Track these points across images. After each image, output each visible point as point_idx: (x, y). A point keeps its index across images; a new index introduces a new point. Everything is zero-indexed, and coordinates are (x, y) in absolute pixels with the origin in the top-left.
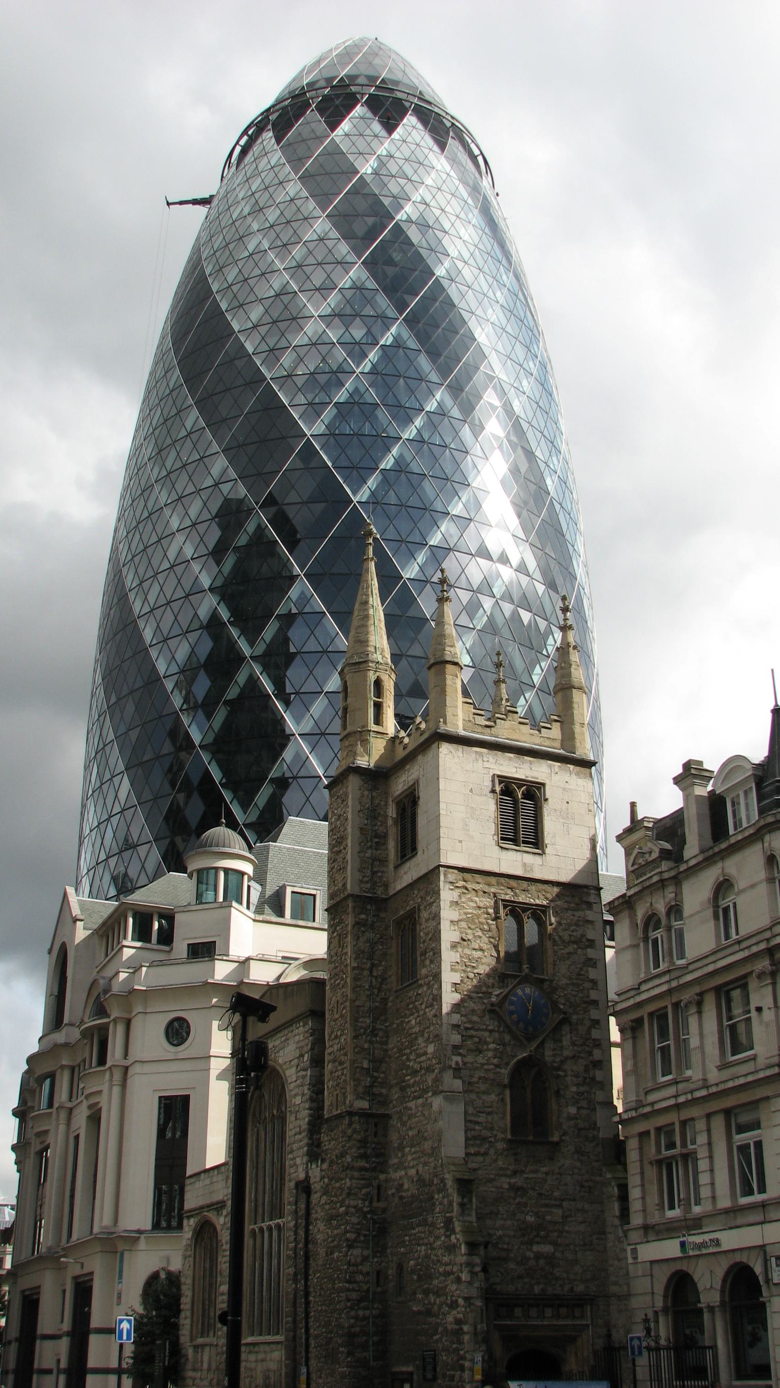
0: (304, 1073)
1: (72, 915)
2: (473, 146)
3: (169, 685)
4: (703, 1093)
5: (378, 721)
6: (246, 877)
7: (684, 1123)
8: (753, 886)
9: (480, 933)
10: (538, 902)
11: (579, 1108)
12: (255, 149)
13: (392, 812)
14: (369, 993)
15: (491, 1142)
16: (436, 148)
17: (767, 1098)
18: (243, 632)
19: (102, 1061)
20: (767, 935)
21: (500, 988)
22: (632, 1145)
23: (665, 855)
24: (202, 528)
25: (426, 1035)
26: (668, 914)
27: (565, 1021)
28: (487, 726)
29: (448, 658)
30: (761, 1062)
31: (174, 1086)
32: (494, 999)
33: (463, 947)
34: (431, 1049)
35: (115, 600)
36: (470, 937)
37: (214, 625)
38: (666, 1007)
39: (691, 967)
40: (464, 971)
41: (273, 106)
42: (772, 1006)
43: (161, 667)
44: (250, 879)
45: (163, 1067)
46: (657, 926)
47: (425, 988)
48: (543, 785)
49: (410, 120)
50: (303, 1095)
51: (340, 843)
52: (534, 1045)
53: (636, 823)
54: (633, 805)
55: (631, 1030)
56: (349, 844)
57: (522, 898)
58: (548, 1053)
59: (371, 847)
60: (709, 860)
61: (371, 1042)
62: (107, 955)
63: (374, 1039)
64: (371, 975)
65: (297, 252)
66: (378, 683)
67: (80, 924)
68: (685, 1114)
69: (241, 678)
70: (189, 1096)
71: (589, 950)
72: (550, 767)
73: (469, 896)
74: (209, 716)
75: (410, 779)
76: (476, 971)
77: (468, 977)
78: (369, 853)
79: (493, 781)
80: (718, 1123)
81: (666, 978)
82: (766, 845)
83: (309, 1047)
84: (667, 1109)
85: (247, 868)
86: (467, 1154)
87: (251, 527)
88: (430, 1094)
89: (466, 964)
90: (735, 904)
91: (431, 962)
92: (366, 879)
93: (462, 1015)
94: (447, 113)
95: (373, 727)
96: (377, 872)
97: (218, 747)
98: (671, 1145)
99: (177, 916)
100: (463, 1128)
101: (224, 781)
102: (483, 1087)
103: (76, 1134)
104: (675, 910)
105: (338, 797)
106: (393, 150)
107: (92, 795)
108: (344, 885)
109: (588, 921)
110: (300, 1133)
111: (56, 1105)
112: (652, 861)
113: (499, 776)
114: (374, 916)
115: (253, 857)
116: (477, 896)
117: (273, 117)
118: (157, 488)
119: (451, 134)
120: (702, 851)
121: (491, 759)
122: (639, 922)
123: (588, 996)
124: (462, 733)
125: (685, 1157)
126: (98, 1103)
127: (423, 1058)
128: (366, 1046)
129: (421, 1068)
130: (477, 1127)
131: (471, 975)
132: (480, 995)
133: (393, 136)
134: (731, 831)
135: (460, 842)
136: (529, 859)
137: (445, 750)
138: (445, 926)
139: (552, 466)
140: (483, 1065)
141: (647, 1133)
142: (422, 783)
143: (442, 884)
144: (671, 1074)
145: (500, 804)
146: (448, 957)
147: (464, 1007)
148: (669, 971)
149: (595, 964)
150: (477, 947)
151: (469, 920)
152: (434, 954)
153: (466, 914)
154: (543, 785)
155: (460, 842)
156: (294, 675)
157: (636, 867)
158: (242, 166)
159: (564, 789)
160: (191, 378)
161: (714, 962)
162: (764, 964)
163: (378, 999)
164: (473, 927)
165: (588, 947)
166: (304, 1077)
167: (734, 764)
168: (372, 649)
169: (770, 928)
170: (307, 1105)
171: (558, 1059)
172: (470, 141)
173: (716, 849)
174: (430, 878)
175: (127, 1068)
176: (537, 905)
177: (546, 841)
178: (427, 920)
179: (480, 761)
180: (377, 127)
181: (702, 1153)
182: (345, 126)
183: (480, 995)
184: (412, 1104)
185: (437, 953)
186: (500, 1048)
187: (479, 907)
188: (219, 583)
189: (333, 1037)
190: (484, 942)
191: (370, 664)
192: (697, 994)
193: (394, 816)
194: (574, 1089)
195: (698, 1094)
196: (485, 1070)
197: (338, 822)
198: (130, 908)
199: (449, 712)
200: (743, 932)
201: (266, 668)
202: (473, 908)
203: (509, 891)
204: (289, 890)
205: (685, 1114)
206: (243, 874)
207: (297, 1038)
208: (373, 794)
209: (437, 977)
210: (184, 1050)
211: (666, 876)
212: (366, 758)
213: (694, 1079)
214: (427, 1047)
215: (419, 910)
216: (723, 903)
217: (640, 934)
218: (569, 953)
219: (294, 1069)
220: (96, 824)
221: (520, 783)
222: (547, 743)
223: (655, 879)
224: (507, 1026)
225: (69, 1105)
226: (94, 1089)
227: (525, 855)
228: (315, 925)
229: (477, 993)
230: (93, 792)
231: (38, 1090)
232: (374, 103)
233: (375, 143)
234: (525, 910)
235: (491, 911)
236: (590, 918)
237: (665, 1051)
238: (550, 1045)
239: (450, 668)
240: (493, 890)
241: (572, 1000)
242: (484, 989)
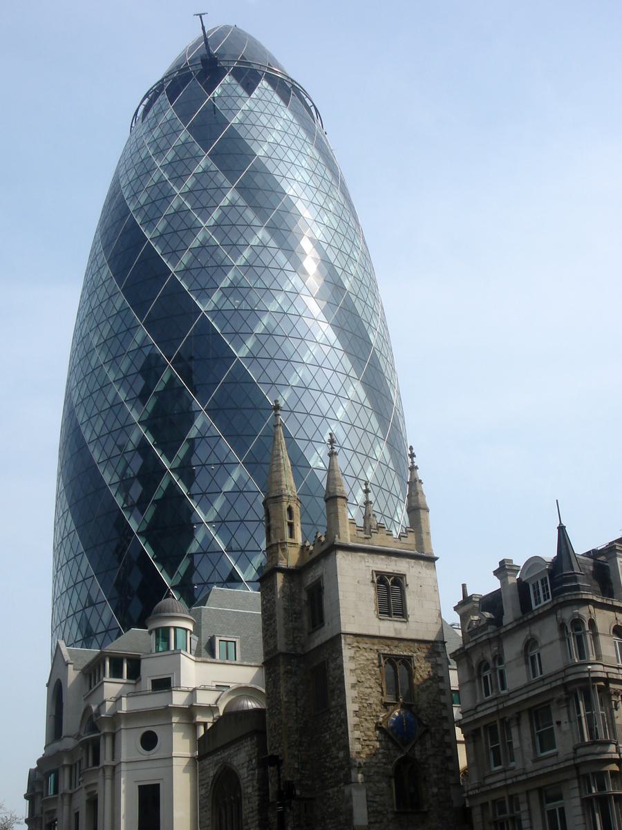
0: (252, 772)
1: (64, 660)
2: (307, 100)
3: (113, 491)
4: (524, 777)
5: (292, 536)
6: (189, 632)
7: (511, 797)
8: (551, 643)
9: (369, 677)
10: (405, 654)
11: (439, 789)
13: (304, 596)
14: (295, 718)
15: (383, 814)
16: (282, 104)
17: (566, 781)
18: (164, 452)
19: (96, 761)
20: (562, 675)
21: (384, 712)
22: (476, 812)
23: (490, 621)
24: (131, 379)
25: (337, 746)
26: (494, 660)
27: (427, 731)
28: (366, 538)
29: (338, 494)
30: (562, 756)
31: (148, 777)
32: (381, 720)
33: (359, 687)
34: (341, 754)
35: (71, 432)
36: (363, 679)
37: (143, 447)
38: (496, 721)
39: (511, 696)
40: (361, 702)
41: (166, 77)
42: (567, 721)
43: (107, 478)
44: (191, 633)
45: (140, 765)
46: (487, 667)
47: (335, 715)
48: (405, 575)
49: (264, 83)
50: (253, 786)
51: (271, 619)
52: (407, 750)
53: (467, 600)
54: (464, 586)
55: (471, 738)
56: (278, 620)
57: (395, 652)
58: (417, 753)
59: (292, 621)
60: (520, 625)
61: (299, 751)
62: (90, 688)
63: (301, 749)
64: (297, 706)
65: (189, 182)
66: (290, 510)
67: (70, 667)
68: (513, 791)
69: (164, 484)
70: (159, 784)
71: (440, 684)
72: (409, 563)
73: (361, 652)
74: (142, 512)
75: (316, 575)
76: (368, 702)
77: (363, 706)
78: (290, 625)
79: (372, 575)
80: (534, 797)
81: (495, 702)
82: (558, 617)
83: (256, 754)
84: (499, 788)
85: (190, 626)
86: (369, 823)
87: (165, 377)
88: (342, 784)
89: (361, 698)
90: (539, 654)
91: (339, 697)
92: (290, 642)
93: (361, 732)
94: (288, 78)
95: (288, 539)
96: (296, 637)
97: (150, 533)
98: (503, 811)
99: (142, 661)
100: (366, 806)
101: (155, 556)
102: (376, 778)
103: (77, 811)
104: (499, 658)
105: (267, 588)
106: (252, 106)
107: (61, 569)
108: (276, 646)
109: (438, 665)
110: (252, 812)
111: (61, 792)
112: (483, 626)
113: (375, 571)
114: (297, 666)
115: (192, 619)
116: (366, 652)
118: (97, 351)
120: (516, 620)
121: (370, 561)
122: (474, 666)
123: (441, 714)
124: (351, 544)
125: (513, 819)
126: (95, 791)
127: (336, 760)
128: (296, 753)
129: (335, 767)
130: (375, 805)
131: (365, 705)
132: (372, 718)
133: (252, 96)
134: (534, 607)
135: (353, 617)
136: (398, 625)
137: (341, 557)
138: (347, 674)
139: (373, 325)
140: (376, 763)
141: (487, 804)
142: (325, 578)
143: (343, 645)
144: (500, 764)
145: (378, 589)
146: (350, 693)
147: (362, 726)
148: (496, 698)
149: (444, 692)
150: (368, 686)
151: (362, 669)
152: (340, 692)
153: (360, 664)
154: (405, 575)
155: (353, 617)
156: (202, 480)
157: (470, 629)
159: (418, 578)
160: (118, 274)
161: (527, 692)
162: (561, 694)
163: (302, 722)
164: (364, 673)
165: (439, 681)
166: (253, 775)
167: (534, 562)
168: (285, 487)
169: (564, 671)
170: (257, 793)
171: (424, 757)
172: (305, 96)
173: (525, 619)
174: (335, 642)
175: (114, 768)
176: (404, 656)
177: (409, 613)
178: (334, 669)
179: (363, 562)
180: (240, 90)
181: (524, 816)
182: (218, 90)
183: (372, 718)
184: (330, 791)
185: (343, 691)
186: (387, 752)
187: (368, 660)
188: (144, 418)
189: (273, 748)
190: (372, 683)
191: (284, 497)
192: (517, 713)
193: (306, 599)
194: (435, 776)
195: (520, 778)
196: (378, 767)
197: (268, 605)
198: (108, 656)
199: (341, 530)
200: (546, 672)
201: (181, 477)
202: (364, 660)
203: (387, 648)
204: (217, 639)
205: (513, 791)
206: (186, 630)
207: (246, 748)
208: (292, 585)
209: (343, 707)
210: (154, 753)
211: (492, 635)
212: (285, 561)
213: (517, 768)
214: (338, 753)
215: (328, 662)
216: (531, 653)
217: (475, 673)
218: (427, 687)
219: (246, 769)
220: (65, 589)
221: (389, 575)
222: (406, 547)
223: (485, 638)
224: (390, 737)
225: (70, 792)
226: (92, 782)
227: (396, 623)
228: (237, 662)
229: (370, 716)
230: (62, 567)
231: (45, 782)
232: (237, 74)
233: (239, 102)
234: (397, 660)
235: (376, 661)
236: (439, 663)
237: (496, 750)
238: (417, 748)
239: (340, 501)
240: (376, 647)
241: (431, 717)
242: (374, 713)
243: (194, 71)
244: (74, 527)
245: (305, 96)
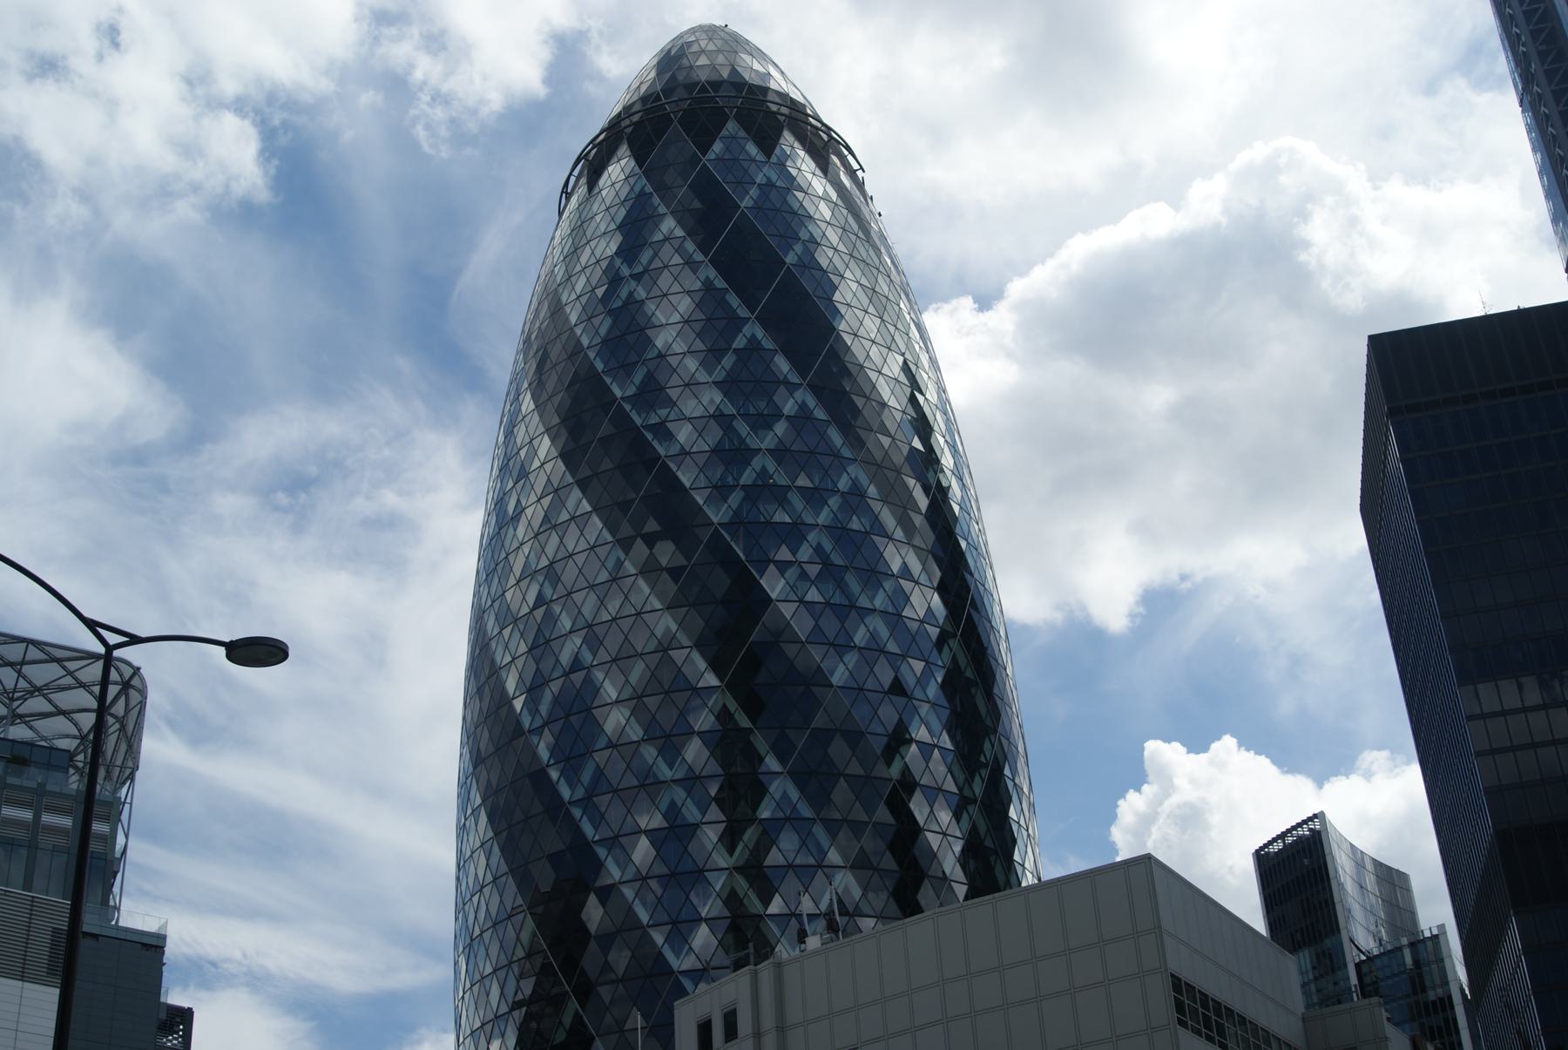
2: (850, 158)
12: (610, 169)
16: (818, 172)
49: (788, 138)
94: (823, 124)
117: (629, 130)
119: (831, 151)
133: (771, 160)
158: (596, 190)
180: (752, 149)
182: (717, 147)
232: (746, 121)
243: (674, 113)
244: (504, 868)
245: (846, 153)
